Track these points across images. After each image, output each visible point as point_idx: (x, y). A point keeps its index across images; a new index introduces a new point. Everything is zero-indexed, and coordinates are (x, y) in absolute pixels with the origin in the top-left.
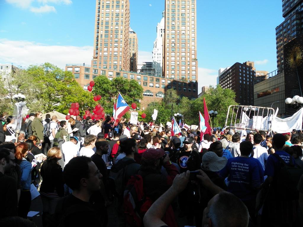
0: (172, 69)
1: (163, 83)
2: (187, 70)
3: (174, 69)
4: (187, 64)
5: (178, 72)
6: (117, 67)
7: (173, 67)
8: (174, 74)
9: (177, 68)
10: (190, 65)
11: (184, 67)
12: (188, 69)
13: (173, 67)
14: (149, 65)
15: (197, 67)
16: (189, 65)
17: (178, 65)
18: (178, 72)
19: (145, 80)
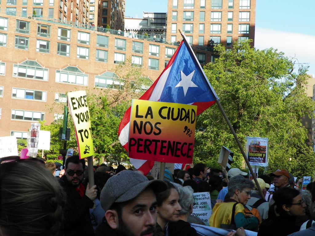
0: (187, 20)
1: (153, 54)
2: (225, 21)
3: (190, 20)
4: (225, 7)
5: (201, 27)
6: (42, 14)
7: (189, 14)
8: (191, 32)
9: (199, 17)
10: (235, 8)
11: (217, 15)
12: (229, 20)
13: (189, 14)
14: (159, 21)
15: (254, 12)
16: (231, 9)
17: (202, 9)
18: (201, 27)
19: (101, 45)
